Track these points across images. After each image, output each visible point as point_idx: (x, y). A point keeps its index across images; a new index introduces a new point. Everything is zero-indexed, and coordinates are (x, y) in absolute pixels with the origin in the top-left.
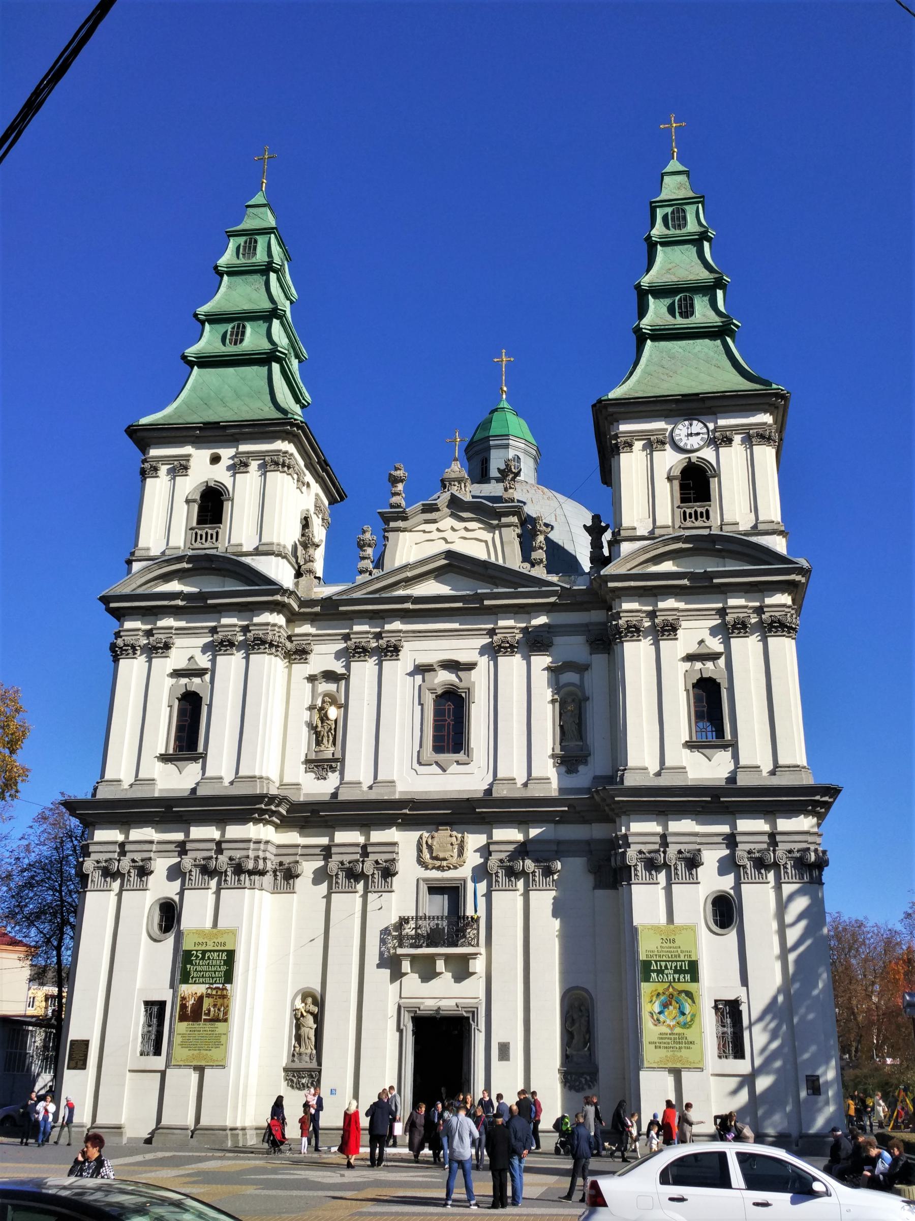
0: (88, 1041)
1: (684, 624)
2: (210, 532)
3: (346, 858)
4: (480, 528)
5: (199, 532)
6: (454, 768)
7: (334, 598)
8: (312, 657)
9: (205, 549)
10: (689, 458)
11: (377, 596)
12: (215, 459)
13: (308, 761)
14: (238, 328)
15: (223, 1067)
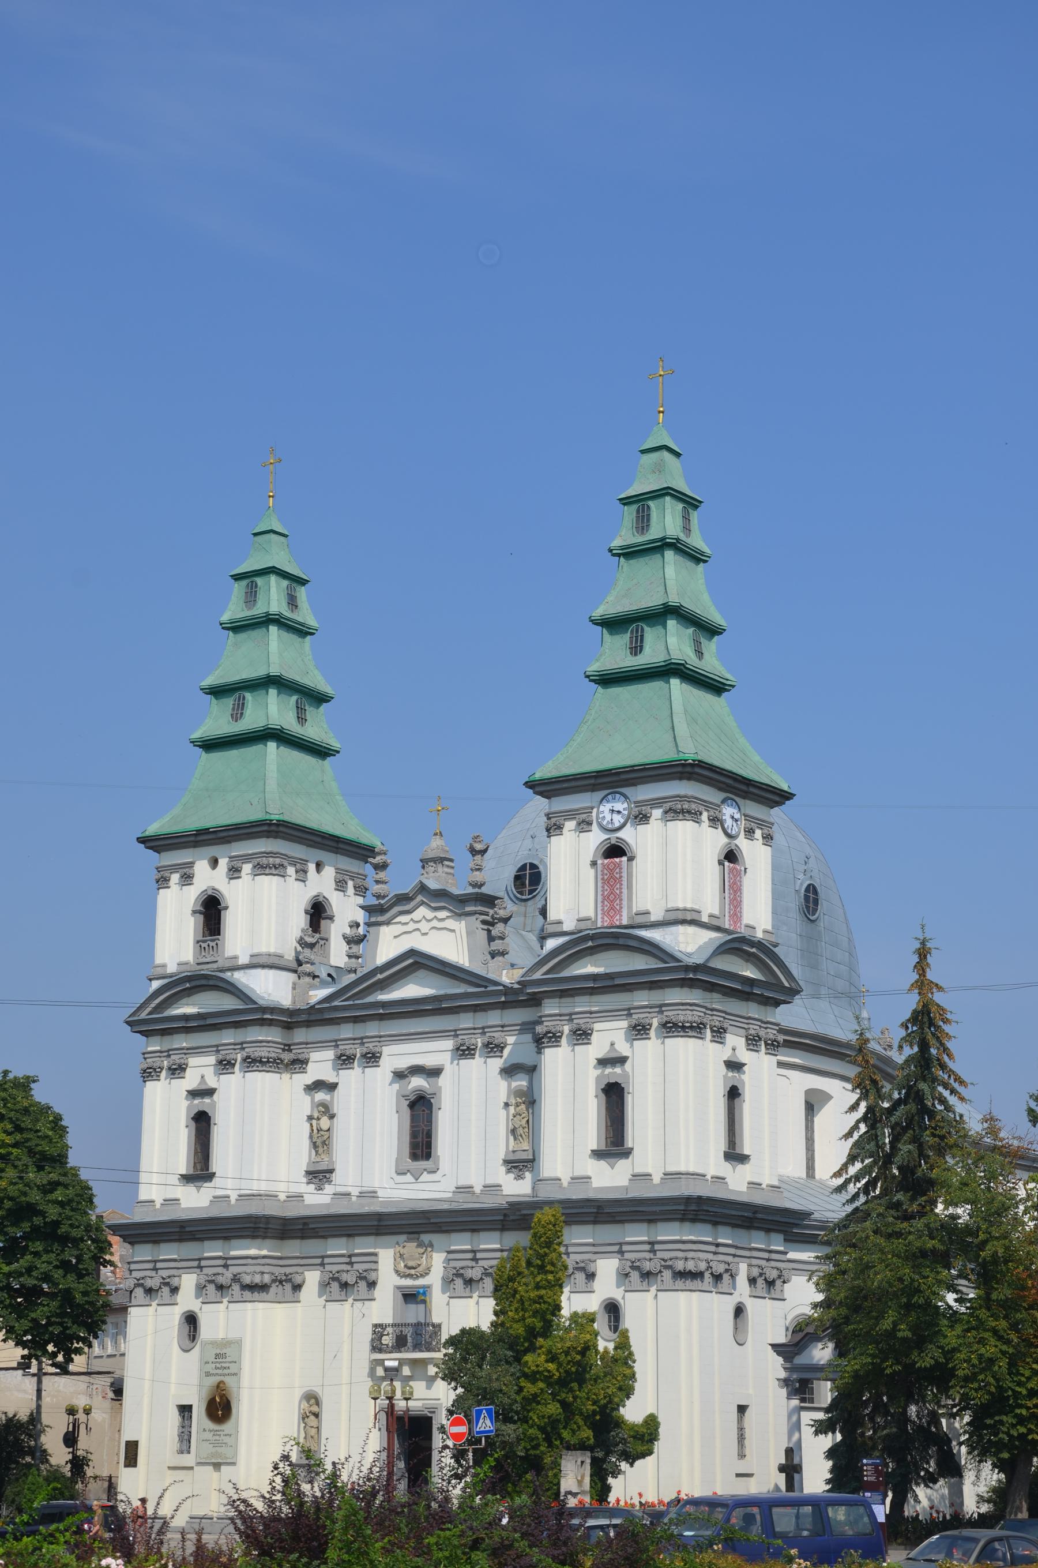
0: (137, 1442)
1: (597, 1026)
2: (211, 944)
3: (335, 1268)
4: (448, 917)
5: (203, 945)
6: (426, 1176)
7: (317, 1007)
8: (310, 1066)
9: (208, 963)
10: (609, 839)
11: (351, 1003)
12: (214, 863)
13: (308, 1173)
14: (239, 697)
15: (234, 1464)
